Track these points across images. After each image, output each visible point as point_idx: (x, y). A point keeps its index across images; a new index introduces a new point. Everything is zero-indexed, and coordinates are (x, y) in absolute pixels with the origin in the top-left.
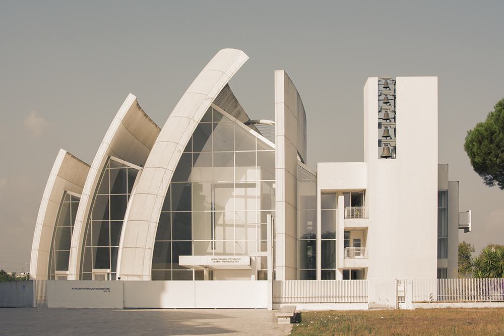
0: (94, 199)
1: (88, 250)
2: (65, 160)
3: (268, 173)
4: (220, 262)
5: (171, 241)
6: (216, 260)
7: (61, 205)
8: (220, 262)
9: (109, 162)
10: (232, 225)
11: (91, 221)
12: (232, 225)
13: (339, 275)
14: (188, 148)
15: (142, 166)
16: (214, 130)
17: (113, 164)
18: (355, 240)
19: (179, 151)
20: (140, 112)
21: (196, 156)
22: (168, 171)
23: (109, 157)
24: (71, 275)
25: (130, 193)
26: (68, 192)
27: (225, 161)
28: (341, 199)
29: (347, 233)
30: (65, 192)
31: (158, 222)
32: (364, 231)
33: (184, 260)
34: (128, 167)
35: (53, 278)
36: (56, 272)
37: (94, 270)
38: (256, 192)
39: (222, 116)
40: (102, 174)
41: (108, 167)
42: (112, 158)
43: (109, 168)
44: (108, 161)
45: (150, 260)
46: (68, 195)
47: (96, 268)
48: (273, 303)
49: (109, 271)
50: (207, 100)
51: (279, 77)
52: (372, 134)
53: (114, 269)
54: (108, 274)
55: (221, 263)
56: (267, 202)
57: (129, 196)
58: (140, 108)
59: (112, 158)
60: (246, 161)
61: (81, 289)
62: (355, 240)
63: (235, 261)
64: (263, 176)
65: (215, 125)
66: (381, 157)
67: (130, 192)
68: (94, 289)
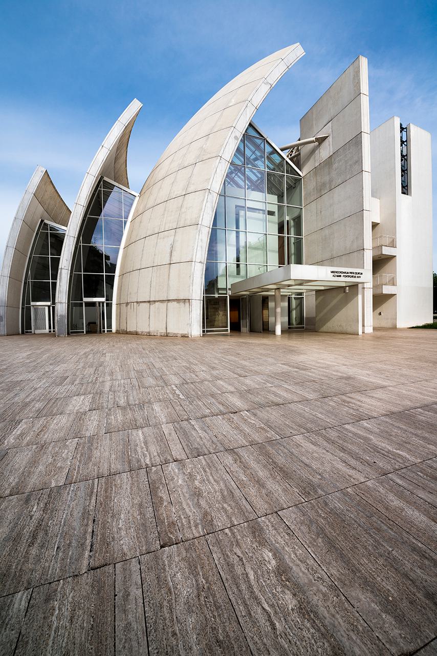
4: (340, 276)
6: (336, 274)
8: (340, 276)
9: (102, 183)
11: (81, 244)
19: (236, 138)
22: (223, 161)
23: (102, 177)
24: (61, 303)
26: (46, 221)
30: (42, 221)
36: (32, 303)
40: (94, 195)
45: (202, 278)
46: (45, 224)
59: (106, 179)
63: (356, 275)
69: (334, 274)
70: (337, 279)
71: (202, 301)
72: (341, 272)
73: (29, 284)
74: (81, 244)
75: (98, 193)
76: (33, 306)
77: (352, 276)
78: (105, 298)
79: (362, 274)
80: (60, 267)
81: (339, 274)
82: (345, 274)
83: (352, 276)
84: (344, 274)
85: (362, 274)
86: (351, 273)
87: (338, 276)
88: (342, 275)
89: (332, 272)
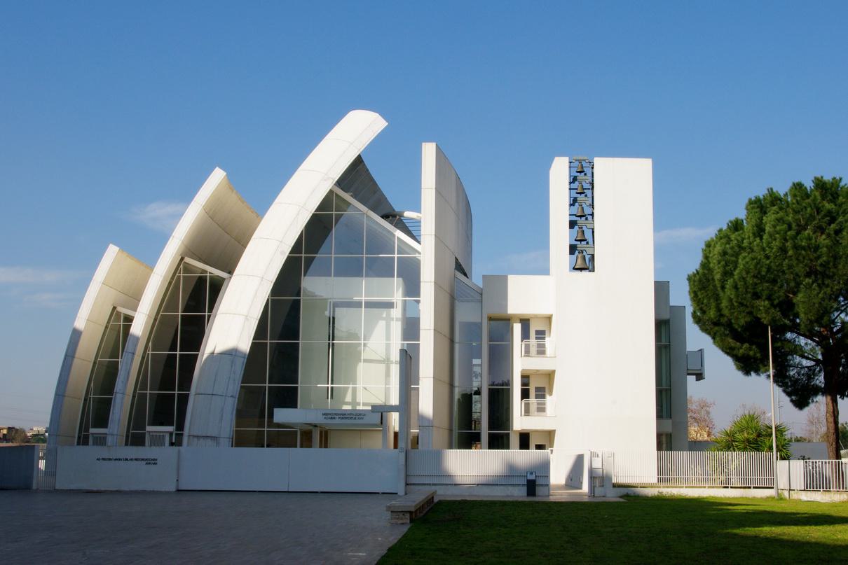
0: (155, 320)
1: (143, 397)
2: (116, 262)
3: (412, 288)
4: (334, 418)
6: (329, 416)
7: (106, 327)
8: (334, 418)
13: (515, 440)
14: (297, 248)
15: (231, 272)
16: (335, 225)
17: (188, 269)
18: (537, 389)
21: (309, 261)
23: (182, 259)
24: (112, 435)
25: (211, 312)
26: (120, 309)
27: (352, 269)
28: (517, 328)
29: (525, 379)
32: (550, 376)
33: (282, 415)
34: (210, 273)
35: (86, 438)
36: (92, 430)
37: (149, 428)
38: (396, 312)
39: (349, 204)
40: (170, 283)
42: (188, 260)
44: (181, 264)
45: (232, 414)
46: (119, 314)
47: (153, 423)
48: (407, 484)
49: (171, 429)
50: (325, 180)
51: (429, 152)
52: (560, 236)
53: (180, 427)
54: (171, 434)
55: (337, 421)
57: (209, 316)
59: (188, 260)
60: (382, 269)
61: (110, 459)
62: (537, 389)
63: (357, 417)
65: (338, 218)
66: (574, 269)
67: (211, 309)
68: (131, 460)
70: (329, 421)
71: (231, 440)
72: (335, 414)
73: (90, 400)
74: (150, 352)
75: (176, 282)
76: (93, 434)
77: (351, 418)
78: (174, 427)
80: (115, 391)
83: (351, 418)
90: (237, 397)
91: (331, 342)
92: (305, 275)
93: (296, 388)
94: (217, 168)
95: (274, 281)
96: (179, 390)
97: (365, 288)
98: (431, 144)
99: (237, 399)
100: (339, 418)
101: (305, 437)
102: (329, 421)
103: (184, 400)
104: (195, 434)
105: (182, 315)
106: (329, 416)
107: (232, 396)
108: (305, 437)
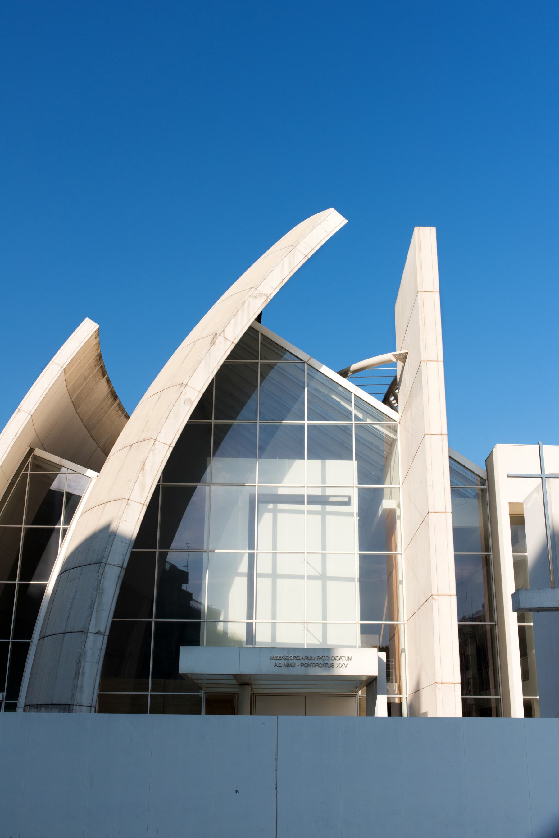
5: (154, 620)
9: (30, 460)
10: (310, 578)
12: (310, 578)
14: (202, 409)
17: (39, 463)
20: (104, 380)
21: (222, 431)
22: (158, 445)
23: (31, 450)
31: (125, 565)
41: (27, 470)
43: (29, 472)
50: (255, 297)
56: (377, 531)
57: (65, 531)
58: (104, 373)
59: (39, 452)
64: (363, 477)
67: (68, 521)
69: (278, 662)
78: (5, 693)
79: (350, 659)
81: (290, 662)
82: (306, 662)
84: (302, 661)
85: (350, 659)
86: (319, 658)
87: (287, 666)
88: (298, 663)
89: (272, 658)
90: (107, 633)
91: (255, 551)
92: (214, 456)
93: (198, 625)
94: (87, 318)
95: (173, 445)
96: (13, 638)
97: (303, 474)
98: (428, 228)
99: (106, 637)
100: (302, 665)
101: (226, 698)
102: (284, 671)
103: (21, 652)
104: (35, 703)
105: (29, 532)
106: (283, 662)
107: (98, 633)
108: (226, 698)
